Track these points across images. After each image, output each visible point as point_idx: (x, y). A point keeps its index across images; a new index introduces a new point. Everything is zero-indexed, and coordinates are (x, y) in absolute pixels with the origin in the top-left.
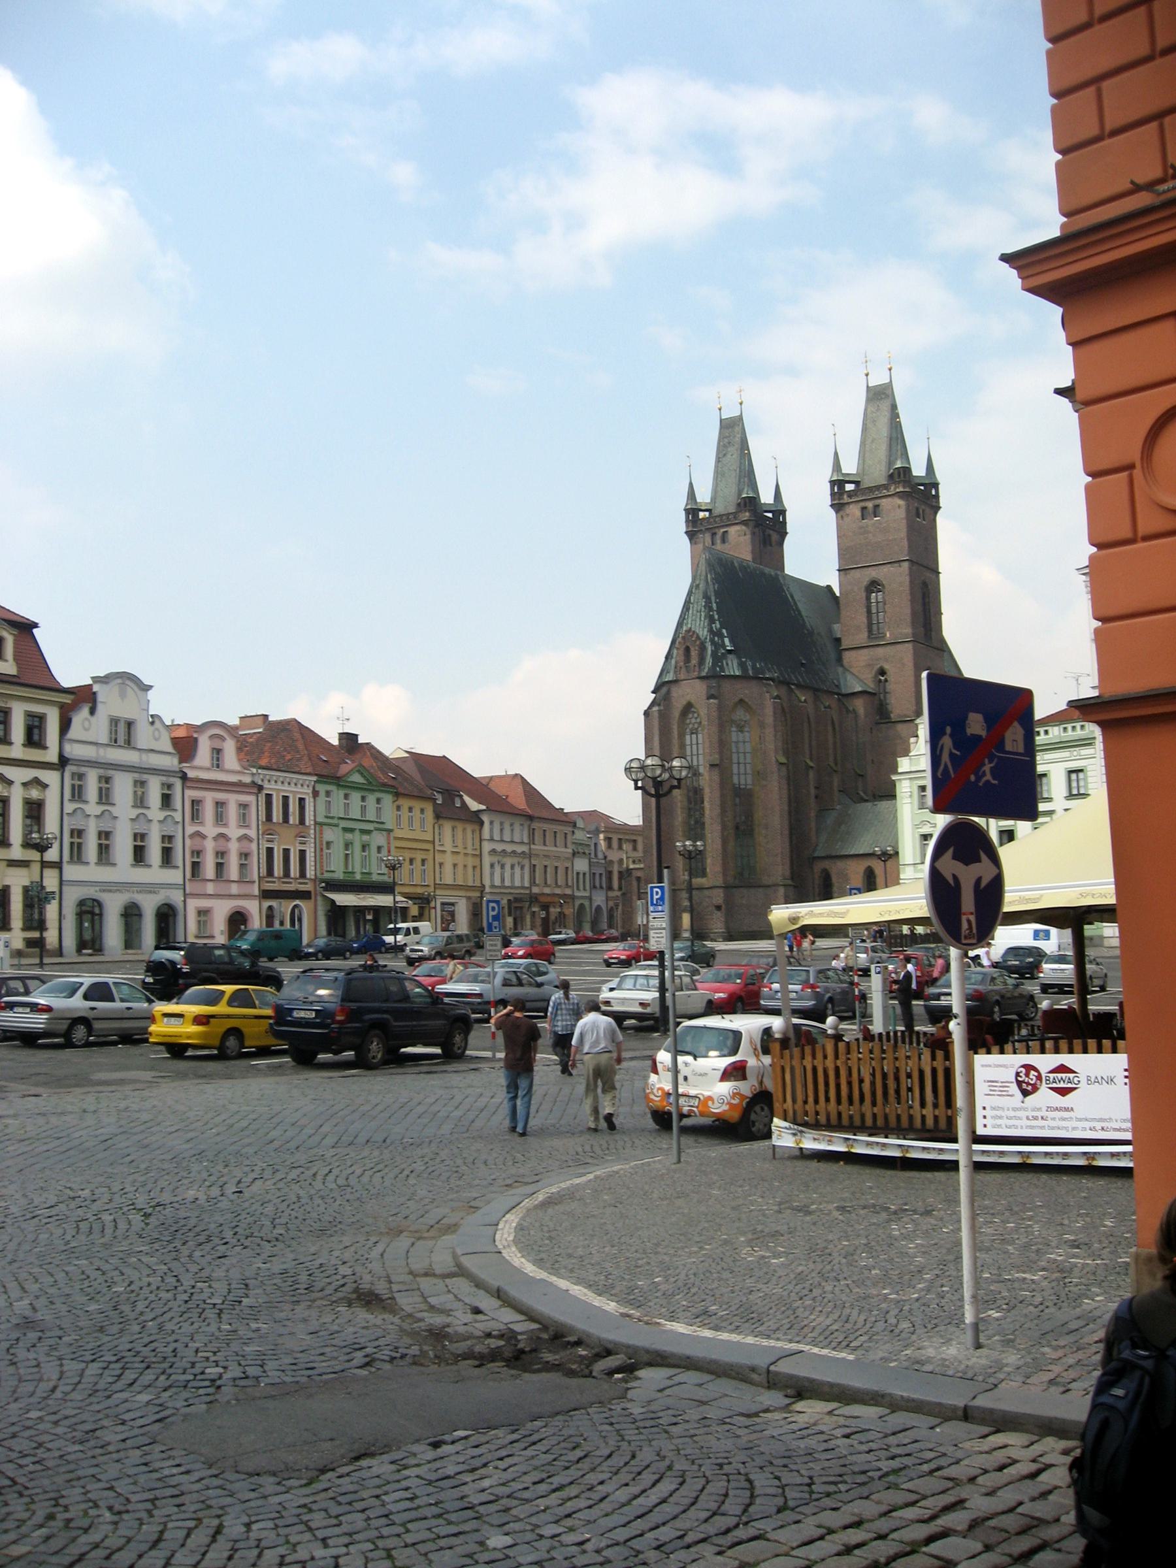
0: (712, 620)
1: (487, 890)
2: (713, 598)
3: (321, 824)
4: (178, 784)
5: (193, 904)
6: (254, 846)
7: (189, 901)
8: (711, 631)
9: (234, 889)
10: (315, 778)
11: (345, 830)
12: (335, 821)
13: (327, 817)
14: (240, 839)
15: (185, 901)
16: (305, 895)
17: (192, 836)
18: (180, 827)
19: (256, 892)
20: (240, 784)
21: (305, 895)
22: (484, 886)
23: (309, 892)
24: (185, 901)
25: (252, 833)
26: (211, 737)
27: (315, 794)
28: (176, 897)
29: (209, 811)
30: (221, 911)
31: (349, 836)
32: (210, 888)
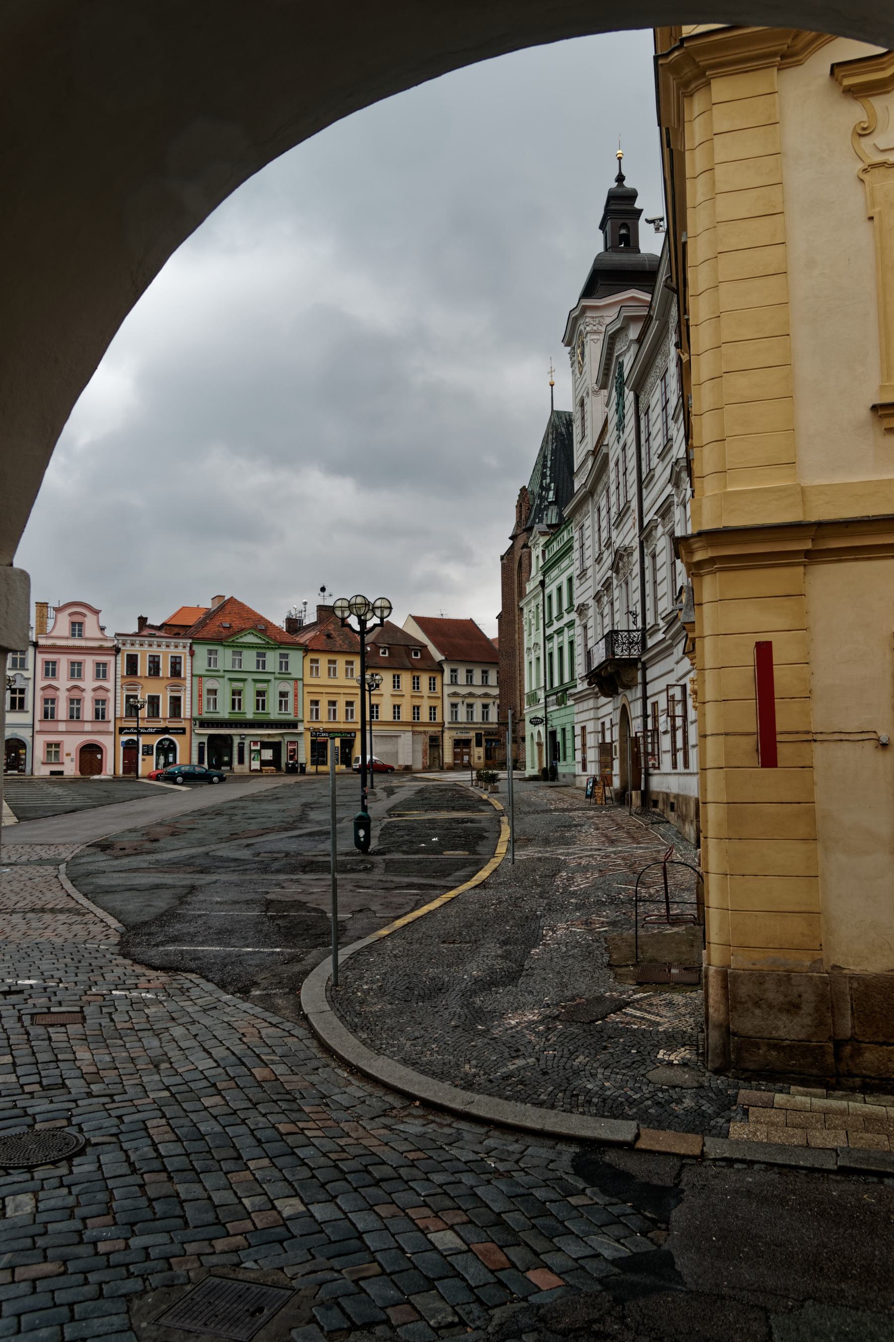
0: (544, 476)
1: (447, 725)
2: (549, 456)
3: (200, 676)
4: (31, 650)
5: (40, 741)
6: (111, 695)
7: (37, 737)
8: (542, 487)
9: (88, 727)
10: (190, 641)
11: (231, 680)
12: (221, 673)
13: (207, 670)
14: (95, 690)
15: (33, 736)
16: (183, 731)
17: (43, 689)
18: (31, 683)
19: (112, 729)
20: (101, 648)
21: (183, 731)
22: (444, 723)
23: (184, 729)
24: (33, 736)
25: (109, 685)
26: (71, 615)
27: (192, 654)
28: (24, 734)
29: (63, 668)
30: (72, 745)
31: (238, 685)
32: (62, 727)
